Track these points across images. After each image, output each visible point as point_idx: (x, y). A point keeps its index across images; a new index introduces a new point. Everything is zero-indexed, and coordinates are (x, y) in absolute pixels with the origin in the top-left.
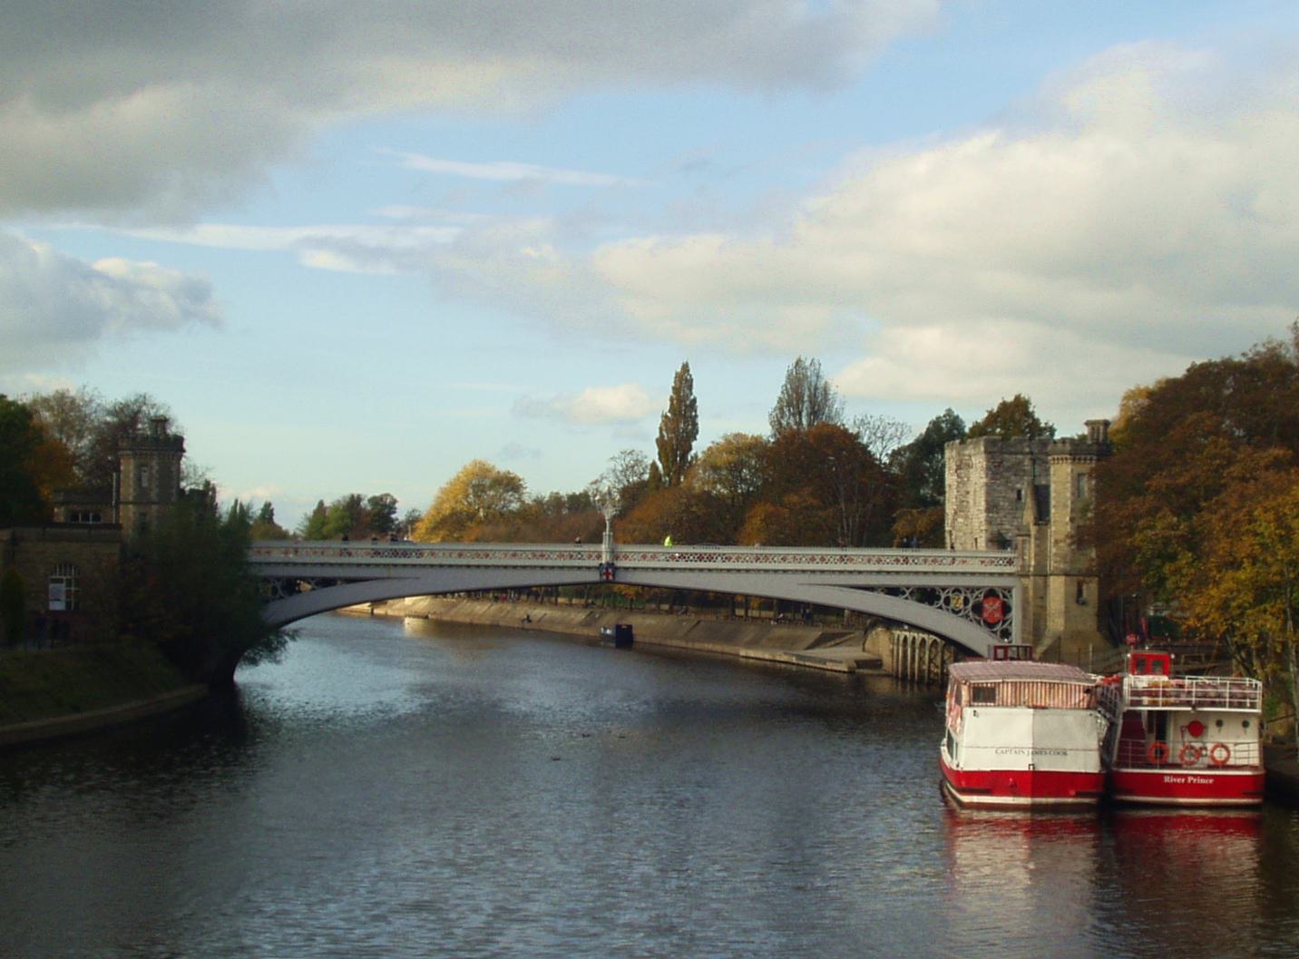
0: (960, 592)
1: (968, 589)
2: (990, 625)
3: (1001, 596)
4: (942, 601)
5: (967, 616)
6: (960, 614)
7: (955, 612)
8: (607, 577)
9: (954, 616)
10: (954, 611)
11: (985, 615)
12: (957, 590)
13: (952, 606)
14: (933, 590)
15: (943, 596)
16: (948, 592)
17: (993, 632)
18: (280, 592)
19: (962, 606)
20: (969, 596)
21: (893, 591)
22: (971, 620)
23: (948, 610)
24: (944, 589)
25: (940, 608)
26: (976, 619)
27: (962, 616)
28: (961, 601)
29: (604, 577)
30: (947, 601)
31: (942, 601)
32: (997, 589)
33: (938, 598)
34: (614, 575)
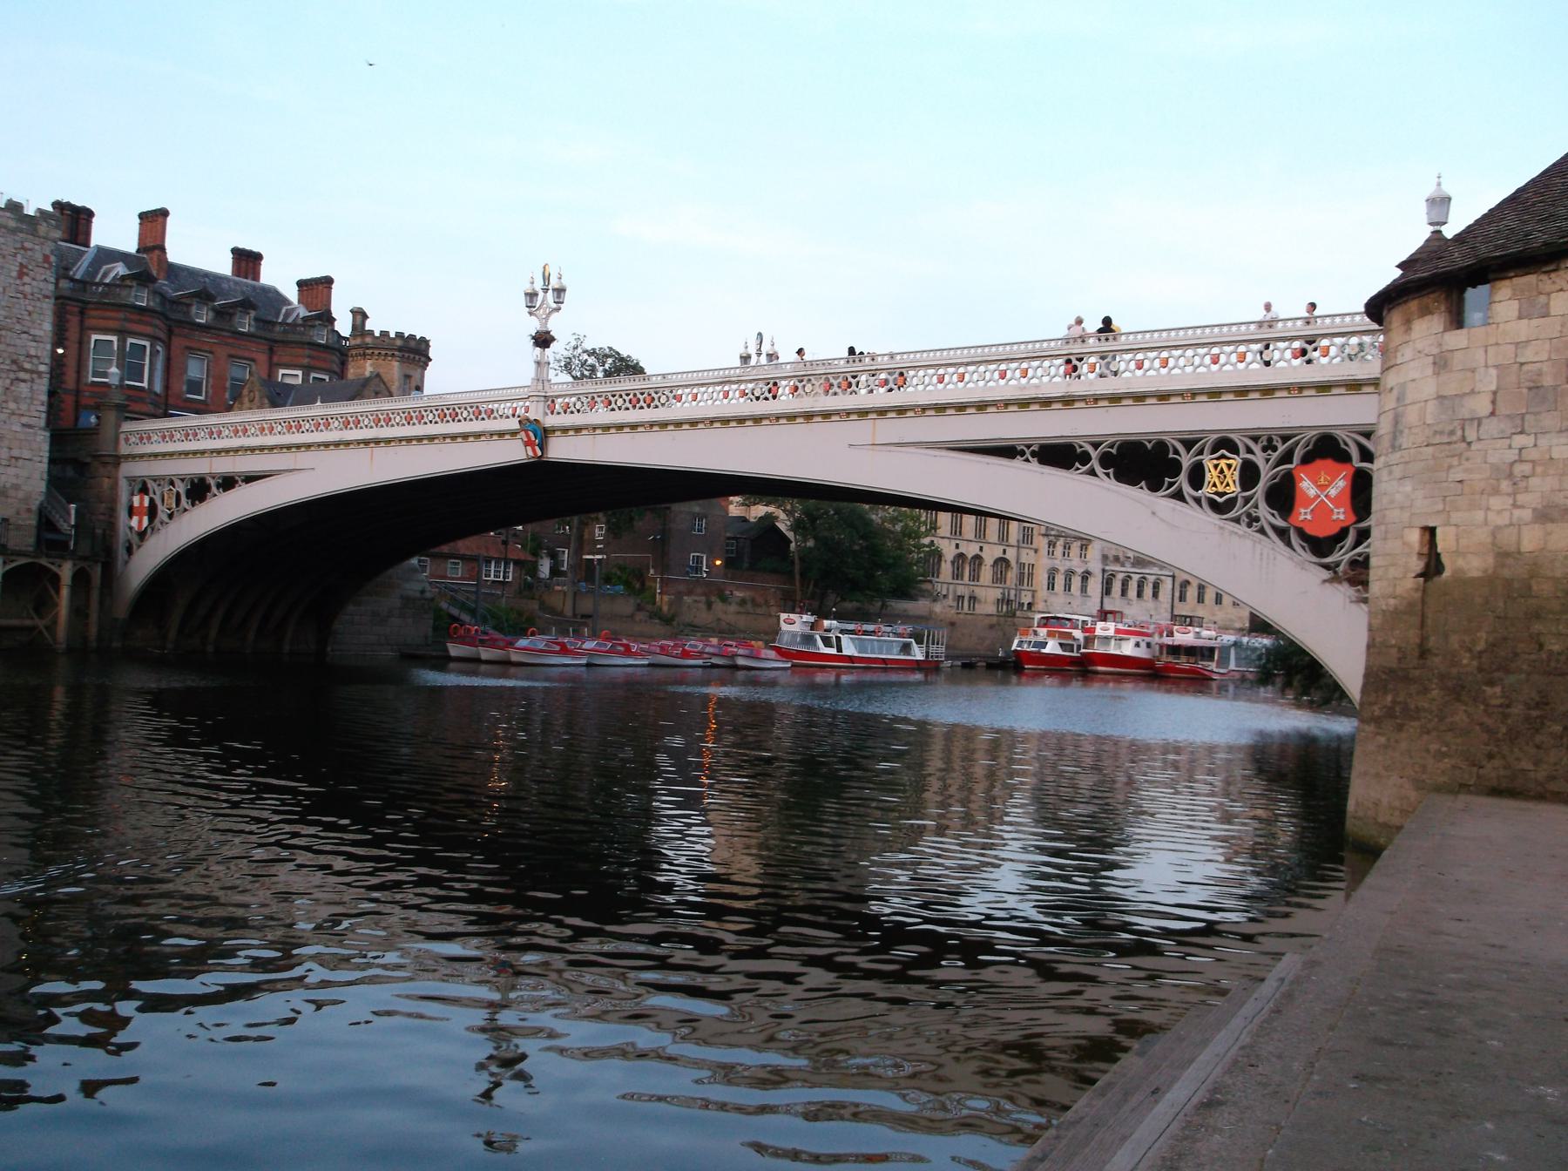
0: (1234, 449)
1: (1256, 439)
2: (1320, 546)
3: (1354, 452)
4: (1183, 480)
5: (1252, 520)
6: (1232, 514)
7: (1220, 507)
8: (534, 451)
9: (1214, 518)
10: (1217, 508)
11: (1303, 514)
12: (1225, 444)
13: (1207, 491)
14: (1161, 446)
15: (1186, 461)
16: (1201, 452)
17: (1327, 567)
18: (183, 498)
19: (1234, 489)
20: (1259, 458)
21: (1059, 455)
22: (1262, 531)
23: (1198, 501)
24: (1189, 444)
25: (1179, 496)
26: (1274, 528)
27: (1237, 520)
28: (1233, 476)
29: (531, 453)
30: (1197, 476)
31: (1183, 480)
32: (1341, 434)
33: (1175, 468)
34: (543, 447)
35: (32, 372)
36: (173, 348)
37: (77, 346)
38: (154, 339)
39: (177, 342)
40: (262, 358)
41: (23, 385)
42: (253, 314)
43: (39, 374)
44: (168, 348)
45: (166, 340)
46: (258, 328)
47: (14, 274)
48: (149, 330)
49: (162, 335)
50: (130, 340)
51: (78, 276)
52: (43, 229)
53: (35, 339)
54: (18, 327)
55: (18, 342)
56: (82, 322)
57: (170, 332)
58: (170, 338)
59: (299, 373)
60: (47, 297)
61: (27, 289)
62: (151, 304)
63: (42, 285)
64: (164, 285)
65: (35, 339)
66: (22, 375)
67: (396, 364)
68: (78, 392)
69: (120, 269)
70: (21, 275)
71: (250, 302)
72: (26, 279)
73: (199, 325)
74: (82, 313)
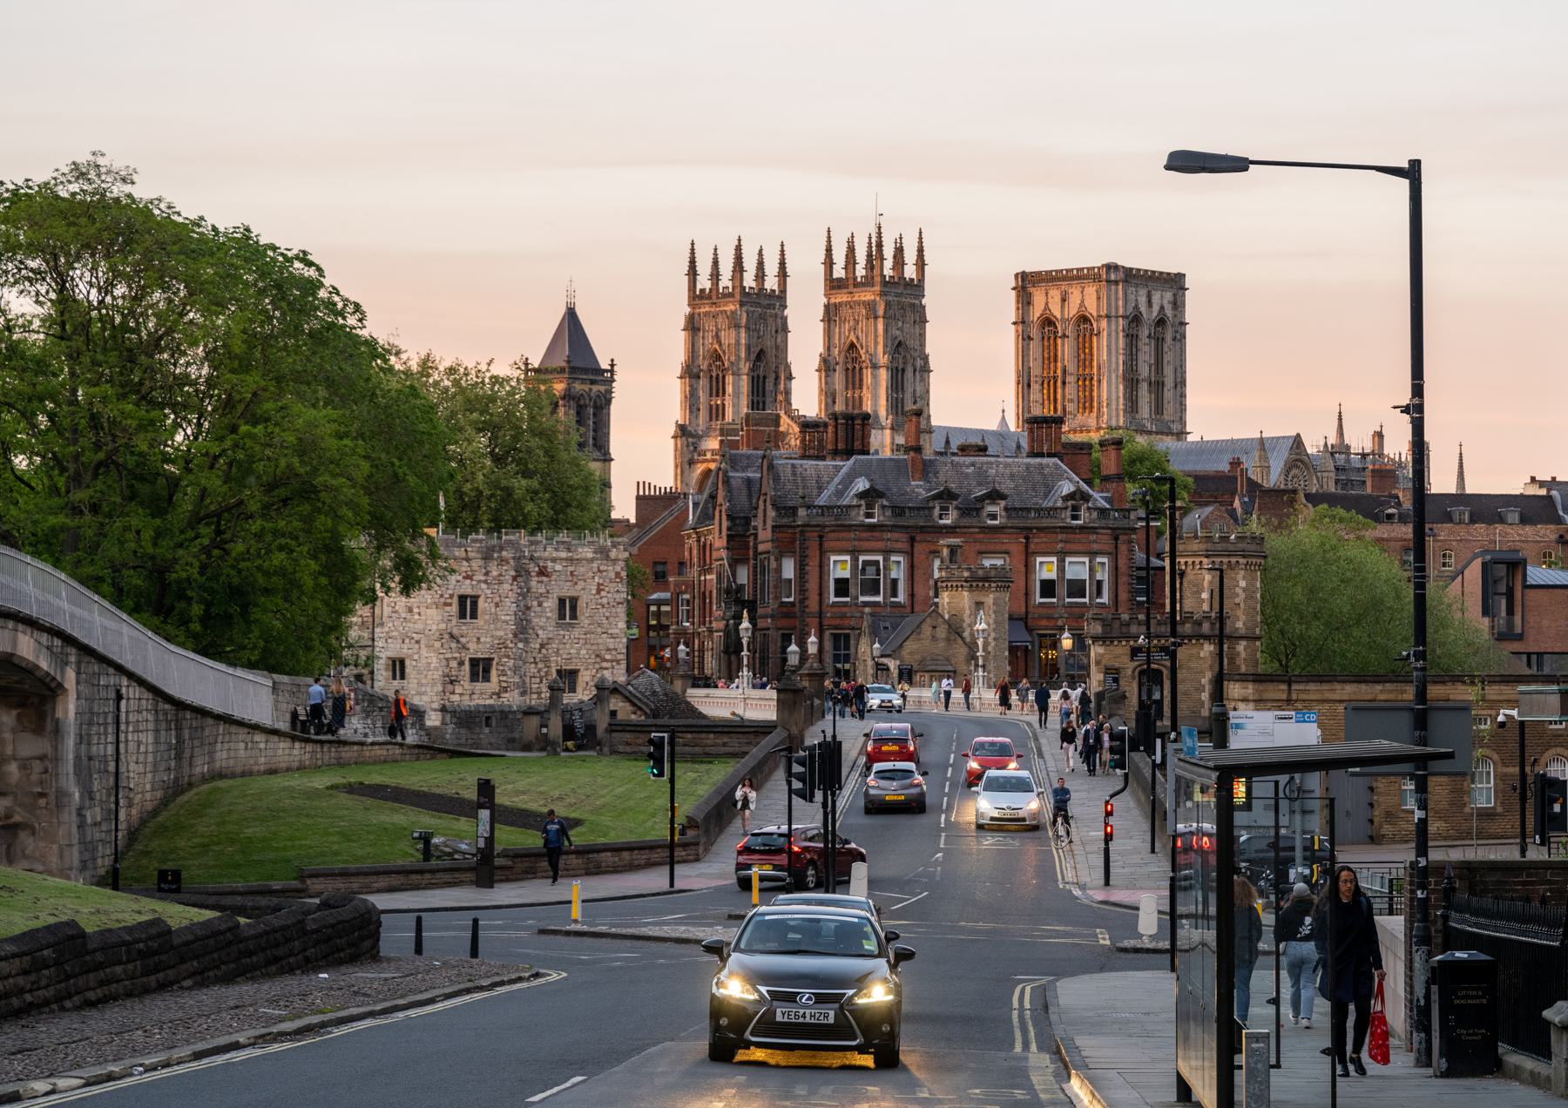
35: (612, 661)
36: (916, 555)
37: (817, 569)
38: (887, 553)
39: (918, 548)
40: (1017, 549)
41: (605, 672)
42: (1003, 503)
43: (618, 662)
44: (910, 555)
45: (909, 549)
46: (1008, 517)
47: (594, 592)
48: (881, 545)
49: (905, 546)
50: (862, 558)
51: (821, 503)
52: (613, 554)
53: (612, 636)
54: (599, 630)
55: (600, 641)
56: (821, 545)
57: (912, 540)
58: (912, 546)
59: (1054, 559)
60: (619, 603)
61: (605, 601)
62: (881, 518)
63: (617, 596)
64: (917, 486)
65: (612, 636)
66: (605, 664)
67: (966, 594)
68: (821, 615)
69: (862, 484)
70: (599, 591)
71: (997, 491)
72: (603, 593)
73: (945, 526)
74: (821, 537)
